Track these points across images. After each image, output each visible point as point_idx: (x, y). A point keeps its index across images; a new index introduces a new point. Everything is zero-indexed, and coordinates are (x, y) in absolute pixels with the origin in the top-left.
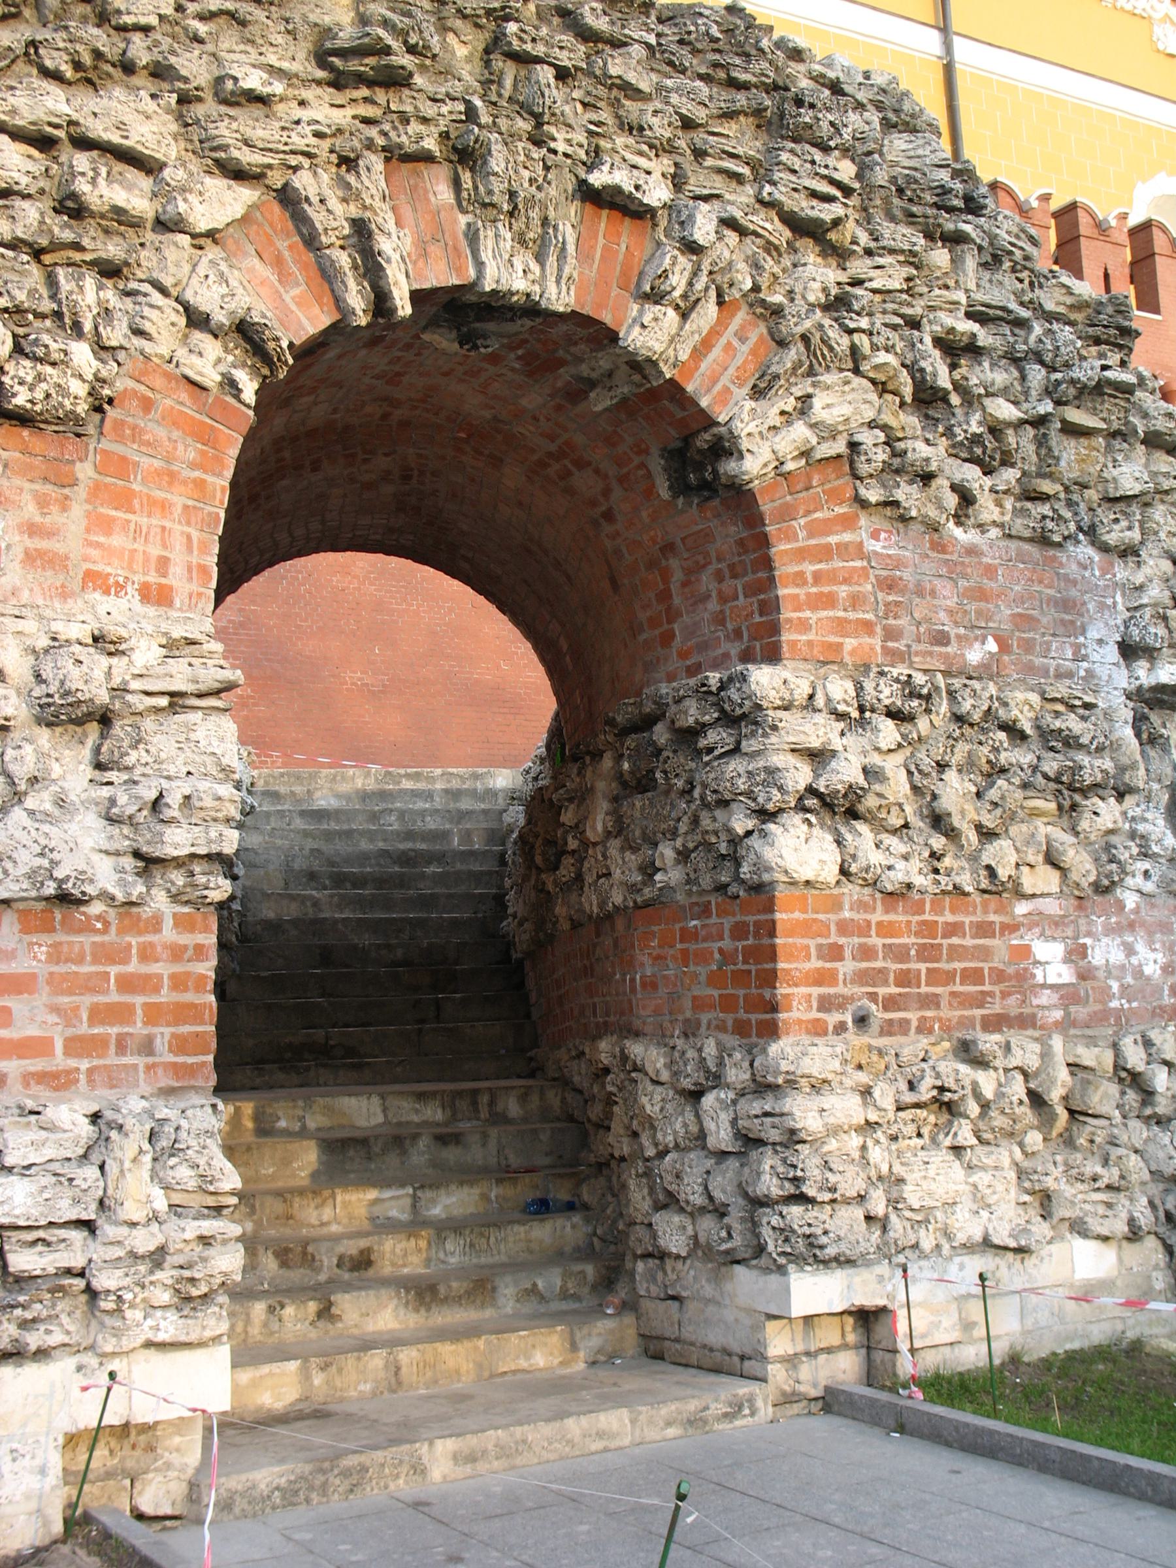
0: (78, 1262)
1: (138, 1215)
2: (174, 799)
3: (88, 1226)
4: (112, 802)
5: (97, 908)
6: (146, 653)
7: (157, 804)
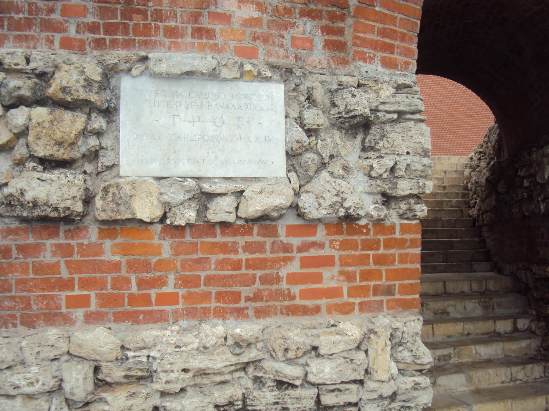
0: (354, 400)
1: (385, 377)
2: (402, 166)
3: (361, 382)
4: (372, 167)
5: (363, 222)
6: (387, 92)
7: (392, 170)
